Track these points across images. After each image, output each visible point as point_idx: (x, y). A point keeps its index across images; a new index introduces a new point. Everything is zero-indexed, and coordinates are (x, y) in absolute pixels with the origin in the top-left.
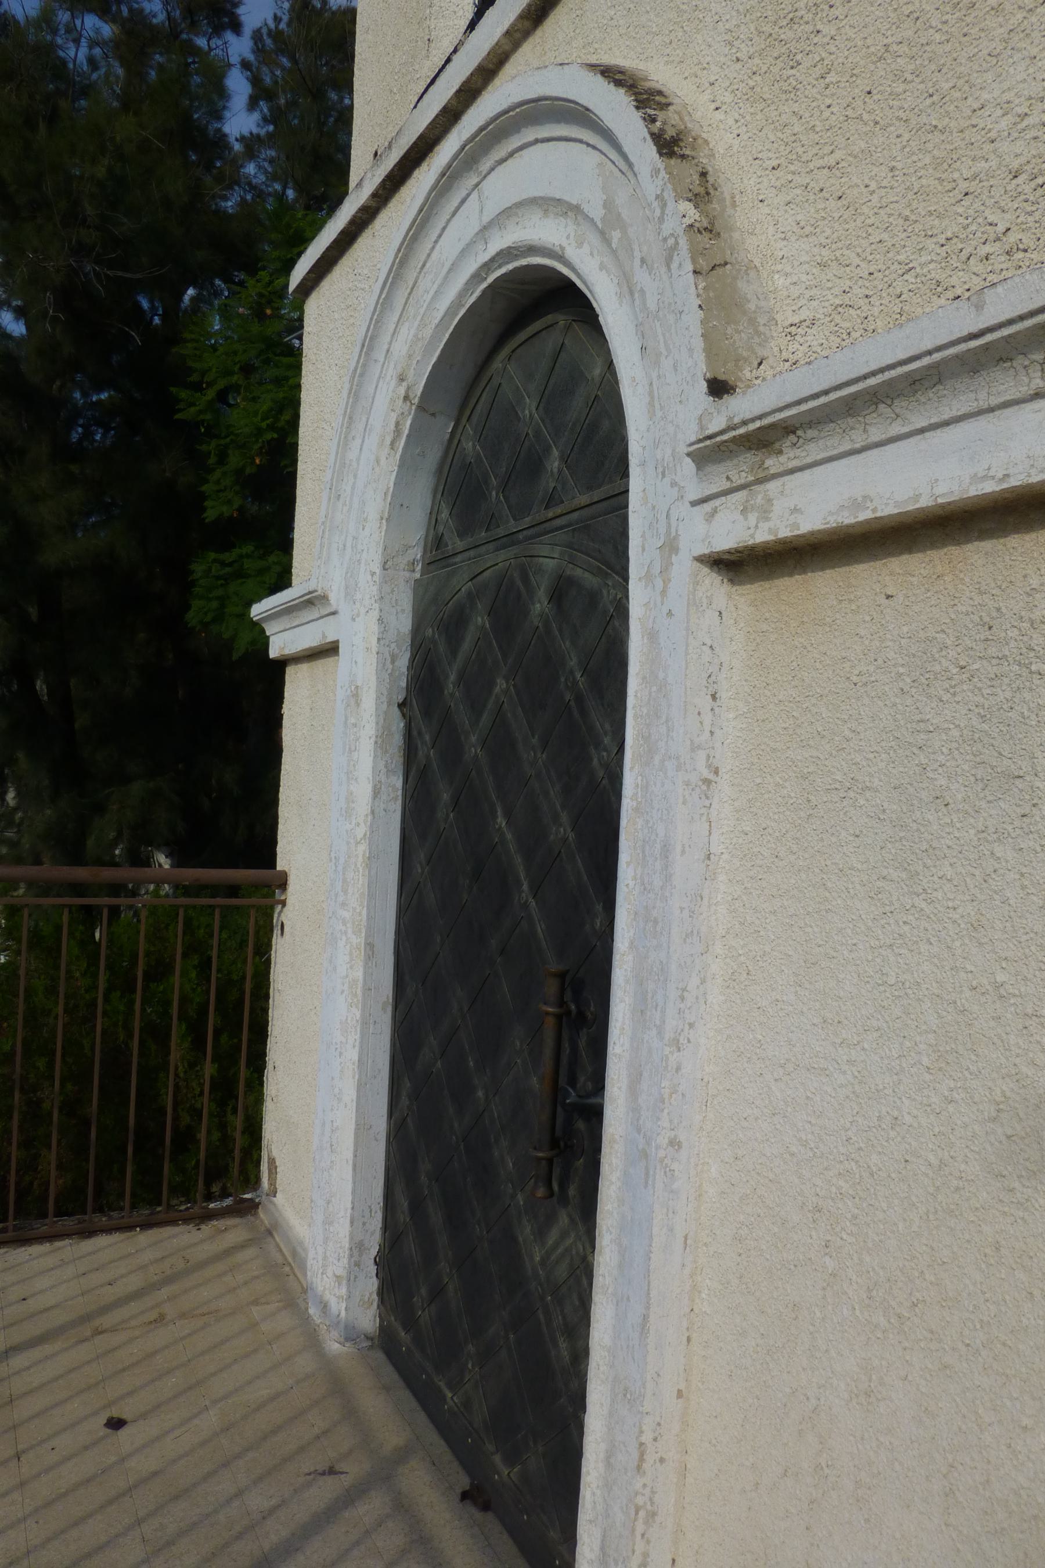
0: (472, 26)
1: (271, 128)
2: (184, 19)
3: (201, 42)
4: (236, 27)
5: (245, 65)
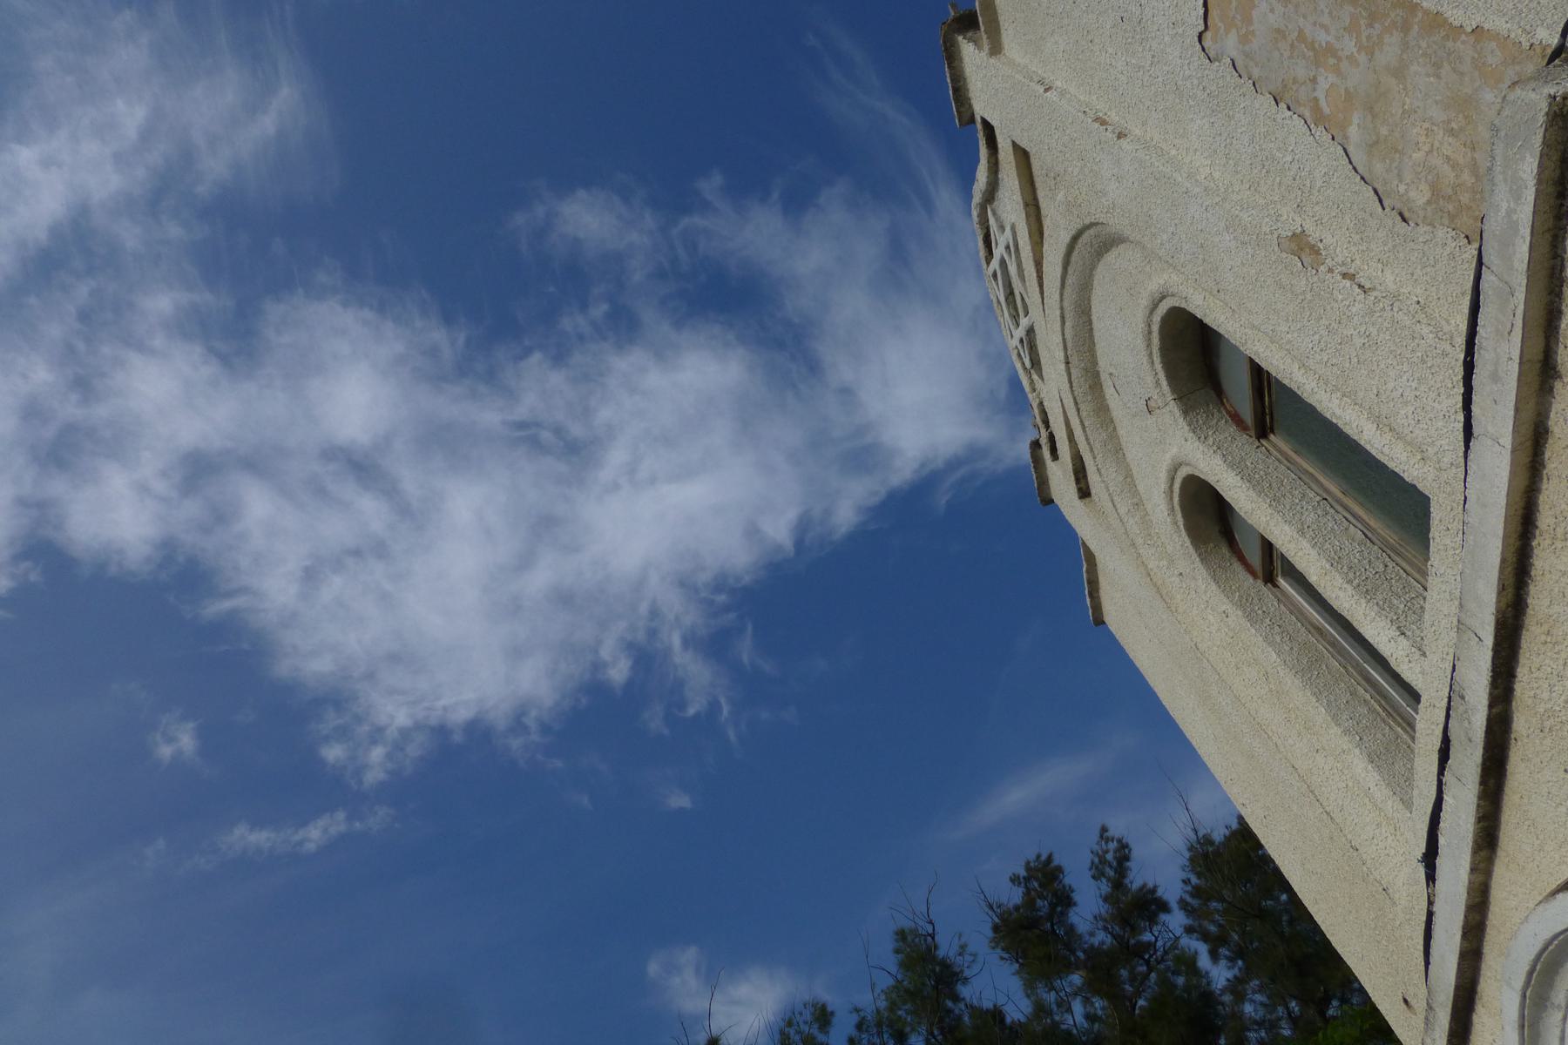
0: (1431, 877)
1: (1240, 963)
3: (1147, 937)
4: (1164, 907)
5: (1189, 930)
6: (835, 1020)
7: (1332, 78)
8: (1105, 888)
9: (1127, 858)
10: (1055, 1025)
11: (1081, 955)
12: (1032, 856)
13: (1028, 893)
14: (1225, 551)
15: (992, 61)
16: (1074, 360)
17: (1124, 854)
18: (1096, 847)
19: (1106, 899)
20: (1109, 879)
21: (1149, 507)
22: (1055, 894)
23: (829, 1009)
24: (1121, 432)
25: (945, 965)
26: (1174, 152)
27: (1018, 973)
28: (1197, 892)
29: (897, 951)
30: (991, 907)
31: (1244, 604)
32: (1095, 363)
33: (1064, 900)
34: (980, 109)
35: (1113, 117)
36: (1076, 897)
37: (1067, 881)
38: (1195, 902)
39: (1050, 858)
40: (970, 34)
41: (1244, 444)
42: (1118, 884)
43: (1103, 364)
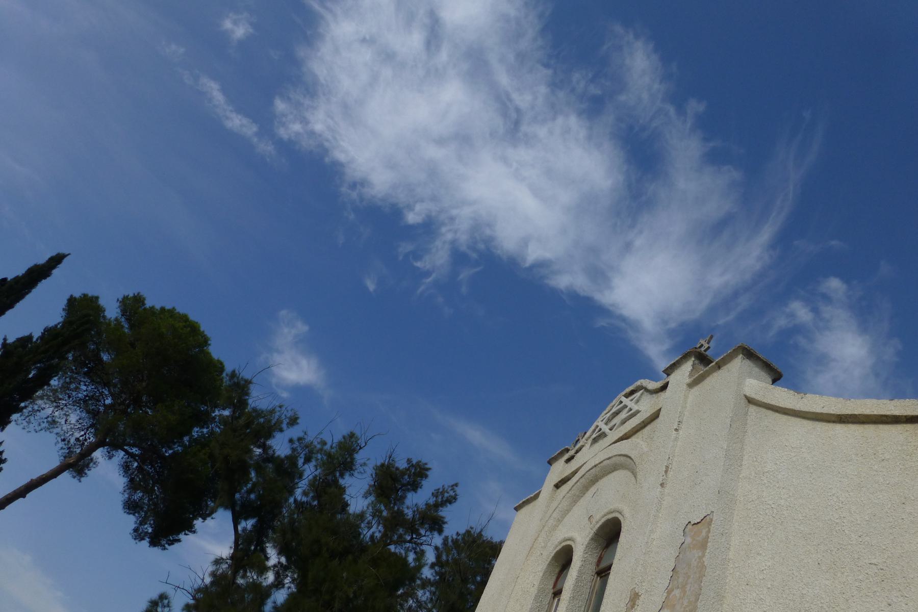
3: (422, 532)
4: (440, 531)
5: (436, 548)
6: (296, 427)
7: (678, 595)
8: (432, 501)
9: (450, 503)
10: (358, 526)
11: (396, 508)
12: (424, 461)
14: (557, 570)
16: (598, 469)
17: (451, 500)
18: (446, 487)
19: (427, 504)
21: (560, 527)
22: (414, 481)
24: (581, 500)
27: (370, 486)
28: (455, 542)
29: (344, 437)
31: (541, 591)
33: (415, 486)
35: (670, 474)
36: (419, 490)
37: (423, 482)
39: (428, 469)
40: (697, 362)
41: (592, 569)
42: (437, 506)
43: (601, 483)
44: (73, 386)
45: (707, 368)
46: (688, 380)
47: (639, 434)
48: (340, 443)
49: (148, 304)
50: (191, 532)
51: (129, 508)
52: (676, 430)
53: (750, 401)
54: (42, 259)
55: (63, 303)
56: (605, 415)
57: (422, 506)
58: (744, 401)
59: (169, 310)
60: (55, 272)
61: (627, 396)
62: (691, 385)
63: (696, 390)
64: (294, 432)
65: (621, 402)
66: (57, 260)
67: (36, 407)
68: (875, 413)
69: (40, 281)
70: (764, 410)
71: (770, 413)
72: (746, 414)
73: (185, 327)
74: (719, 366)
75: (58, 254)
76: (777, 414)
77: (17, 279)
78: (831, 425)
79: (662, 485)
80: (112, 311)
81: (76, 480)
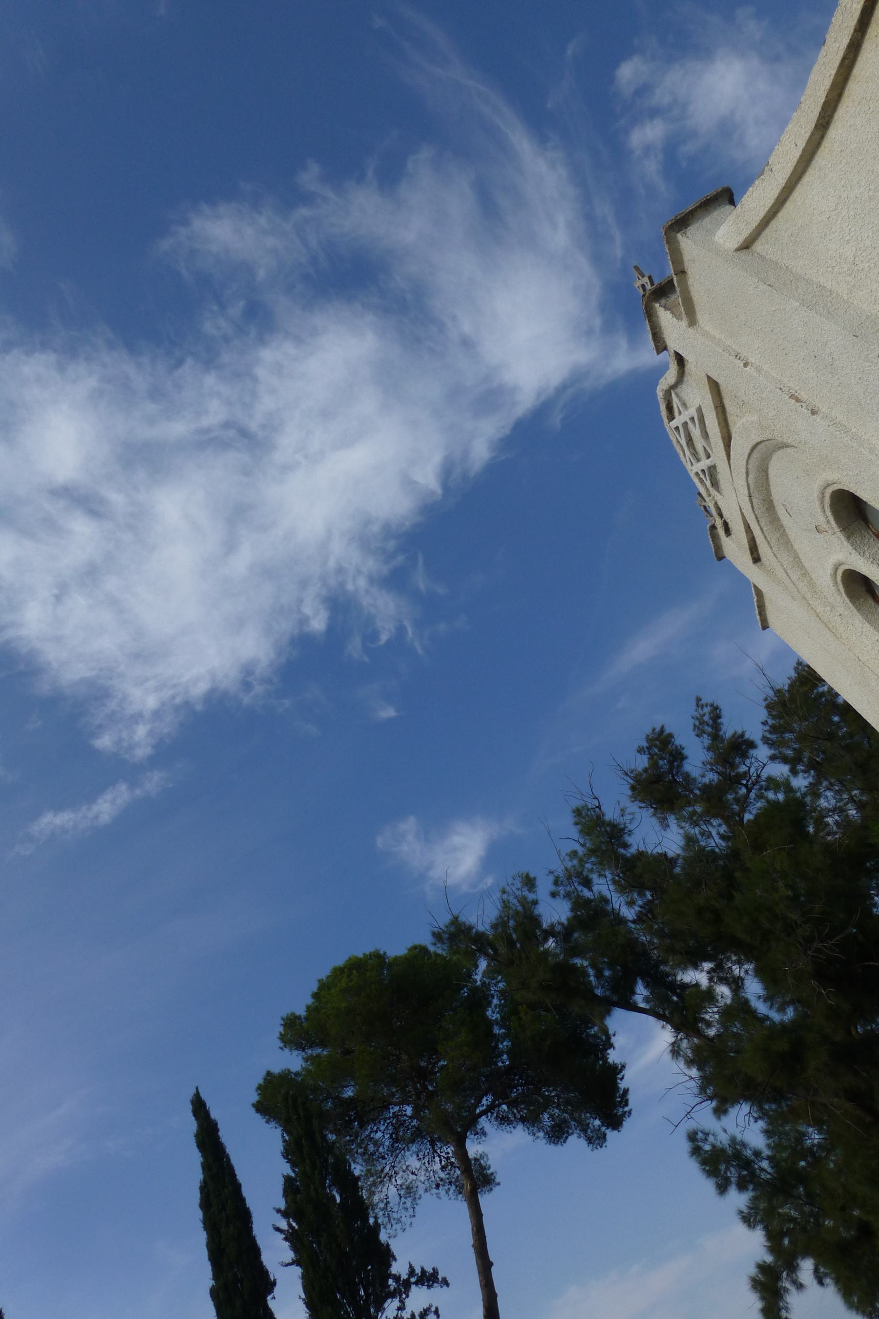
1: (812, 772)
2: (725, 767)
3: (743, 769)
4: (752, 745)
5: (773, 758)
6: (538, 882)
8: (707, 740)
9: (719, 717)
11: (697, 792)
12: (649, 731)
13: (652, 757)
14: (871, 602)
15: (691, 330)
16: (755, 495)
17: (716, 714)
18: (695, 714)
19: (708, 749)
20: (709, 735)
21: (813, 576)
22: (671, 754)
23: (532, 876)
24: (789, 533)
25: (614, 826)
26: (854, 430)
27: (654, 815)
28: (774, 729)
29: (576, 824)
30: (626, 774)
32: (769, 494)
33: (678, 756)
34: (673, 344)
35: (803, 395)
36: (686, 752)
37: (678, 741)
38: (774, 737)
40: (663, 301)
42: (716, 737)
43: (777, 496)
44: (371, 1148)
45: (678, 290)
46: (684, 323)
47: (731, 419)
48: (581, 831)
49: (301, 1012)
50: (621, 1071)
51: (559, 1138)
52: (746, 365)
53: (746, 246)
54: (192, 1125)
55: (258, 1120)
56: (686, 457)
57: (708, 756)
58: (743, 254)
59: (320, 988)
60: (213, 1115)
61: (671, 417)
62: (692, 322)
63: (702, 317)
64: (544, 886)
65: (677, 428)
66: (199, 1107)
67: (382, 1205)
68: (833, 72)
69: (218, 1137)
70: (767, 231)
71: (773, 224)
72: (763, 258)
73: (349, 976)
74: (682, 272)
75: (192, 1102)
76: (780, 214)
77: (206, 1167)
78: (826, 144)
79: (814, 412)
80: (293, 1061)
81: (496, 1190)
